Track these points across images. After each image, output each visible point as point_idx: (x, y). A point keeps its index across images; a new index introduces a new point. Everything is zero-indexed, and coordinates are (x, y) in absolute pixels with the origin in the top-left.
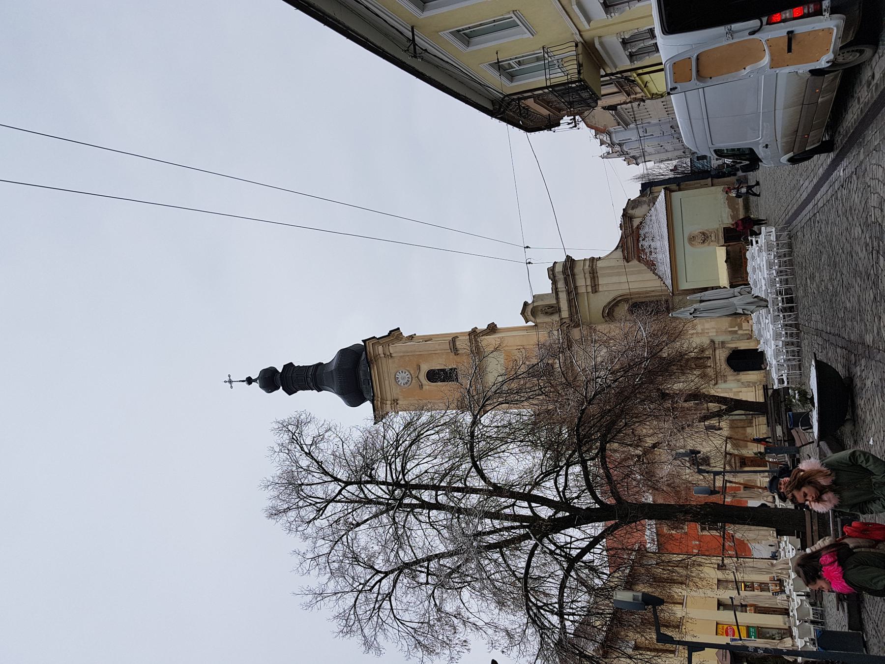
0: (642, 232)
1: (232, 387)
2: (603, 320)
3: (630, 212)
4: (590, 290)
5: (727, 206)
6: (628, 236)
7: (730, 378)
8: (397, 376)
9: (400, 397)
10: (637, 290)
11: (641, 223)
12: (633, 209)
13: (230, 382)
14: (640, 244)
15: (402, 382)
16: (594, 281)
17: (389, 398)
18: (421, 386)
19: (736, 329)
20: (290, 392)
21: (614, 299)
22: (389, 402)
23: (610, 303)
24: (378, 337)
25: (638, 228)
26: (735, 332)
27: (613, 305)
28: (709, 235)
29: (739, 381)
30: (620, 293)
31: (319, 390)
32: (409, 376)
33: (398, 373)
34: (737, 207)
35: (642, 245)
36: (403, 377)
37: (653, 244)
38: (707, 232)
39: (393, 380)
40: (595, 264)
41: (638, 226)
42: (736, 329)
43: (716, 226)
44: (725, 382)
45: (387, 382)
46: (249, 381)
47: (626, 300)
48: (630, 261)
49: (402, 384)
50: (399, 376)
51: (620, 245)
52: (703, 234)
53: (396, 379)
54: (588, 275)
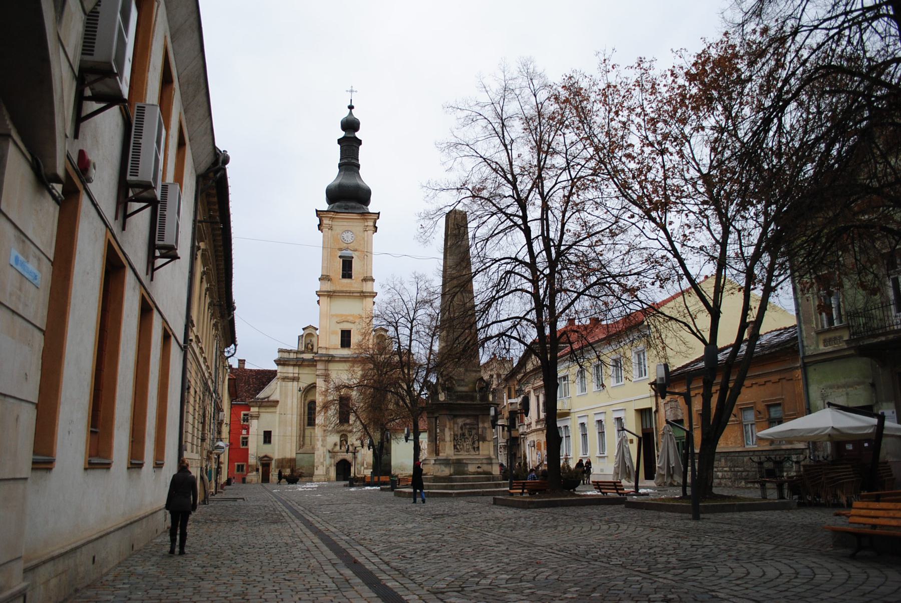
1: (347, 91)
7: (333, 461)
9: (333, 232)
13: (352, 91)
15: (345, 235)
17: (334, 223)
18: (341, 249)
19: (365, 466)
20: (340, 141)
22: (330, 222)
24: (377, 221)
26: (363, 465)
29: (331, 465)
31: (340, 166)
36: (348, 237)
42: (365, 466)
44: (331, 457)
45: (345, 224)
46: (351, 107)
50: (349, 234)
53: (348, 231)
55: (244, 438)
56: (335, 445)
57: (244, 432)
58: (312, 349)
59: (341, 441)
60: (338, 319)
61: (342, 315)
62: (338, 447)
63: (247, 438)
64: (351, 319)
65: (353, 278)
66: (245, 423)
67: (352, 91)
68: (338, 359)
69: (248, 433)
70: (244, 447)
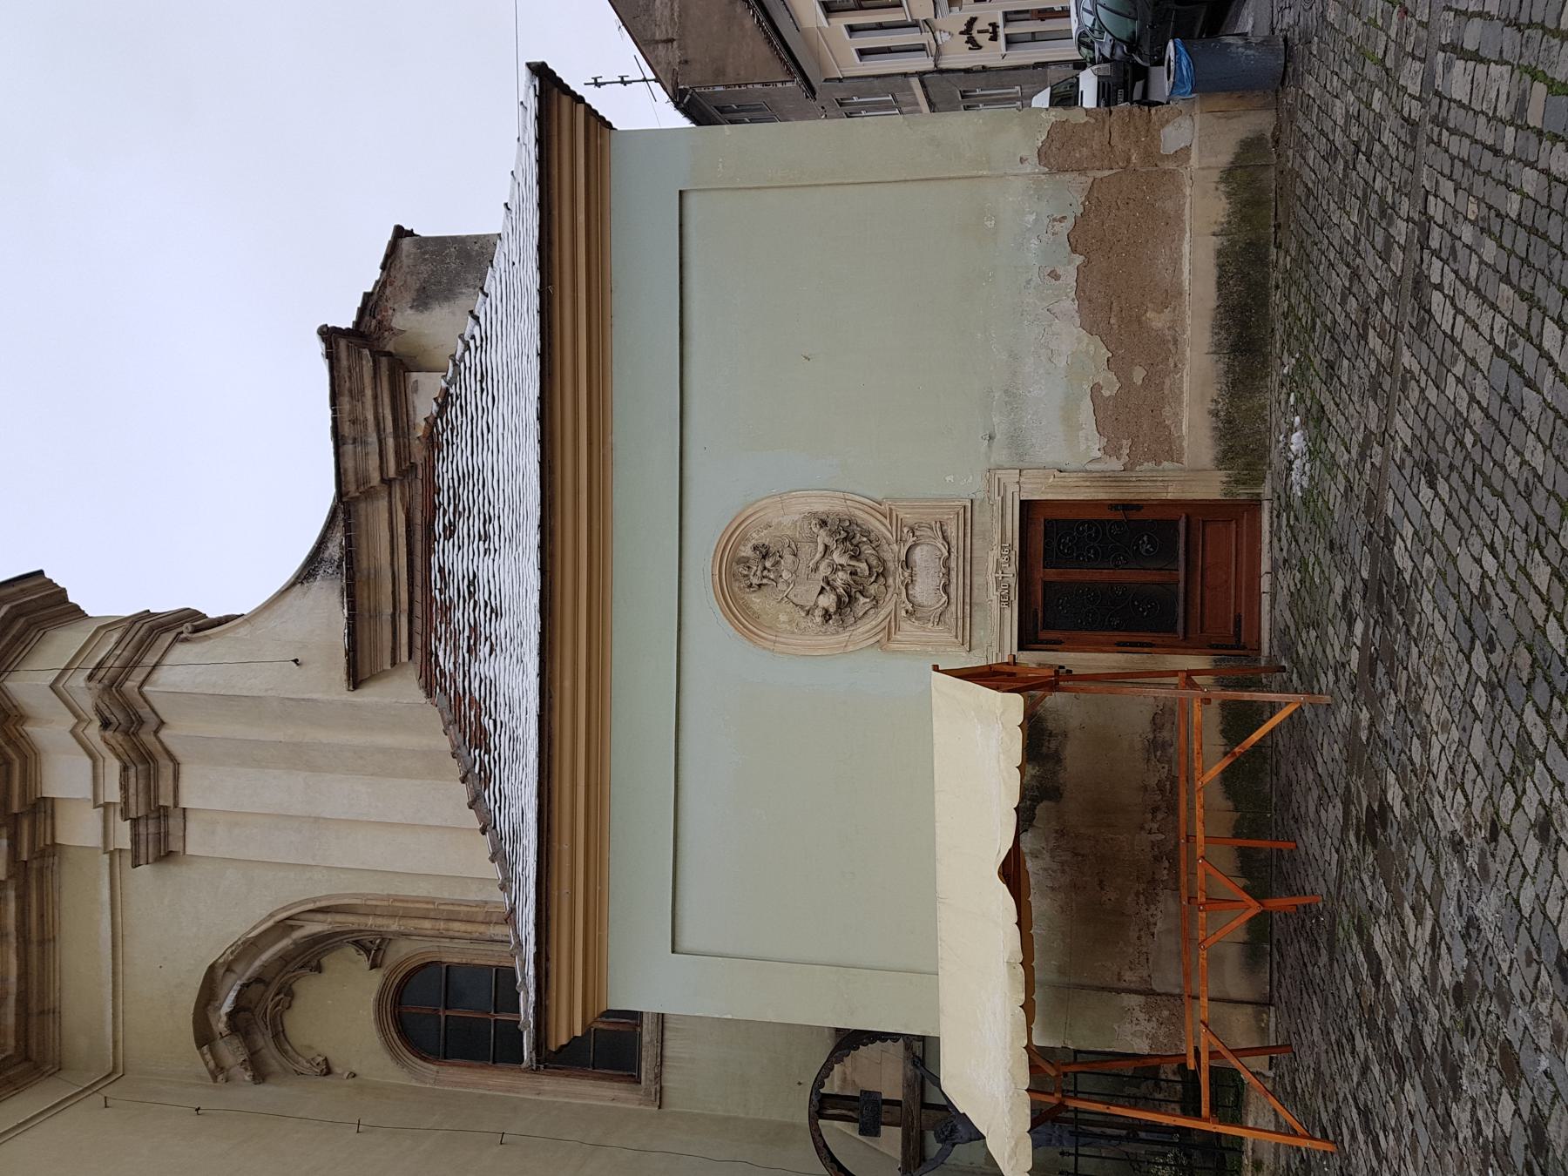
0: (446, 473)
2: (193, 1060)
3: (405, 320)
4: (122, 835)
5: (1069, 305)
6: (369, 494)
10: (423, 890)
11: (444, 401)
12: (423, 300)
14: (434, 560)
16: (151, 789)
21: (285, 926)
23: (249, 947)
25: (433, 442)
27: (284, 959)
28: (893, 553)
30: (322, 889)
34: (1157, 320)
35: (441, 570)
37: (485, 568)
38: (876, 525)
40: (150, 659)
41: (431, 423)
43: (965, 483)
47: (373, 948)
48: (376, 676)
51: (334, 550)
52: (848, 534)
54: (93, 732)
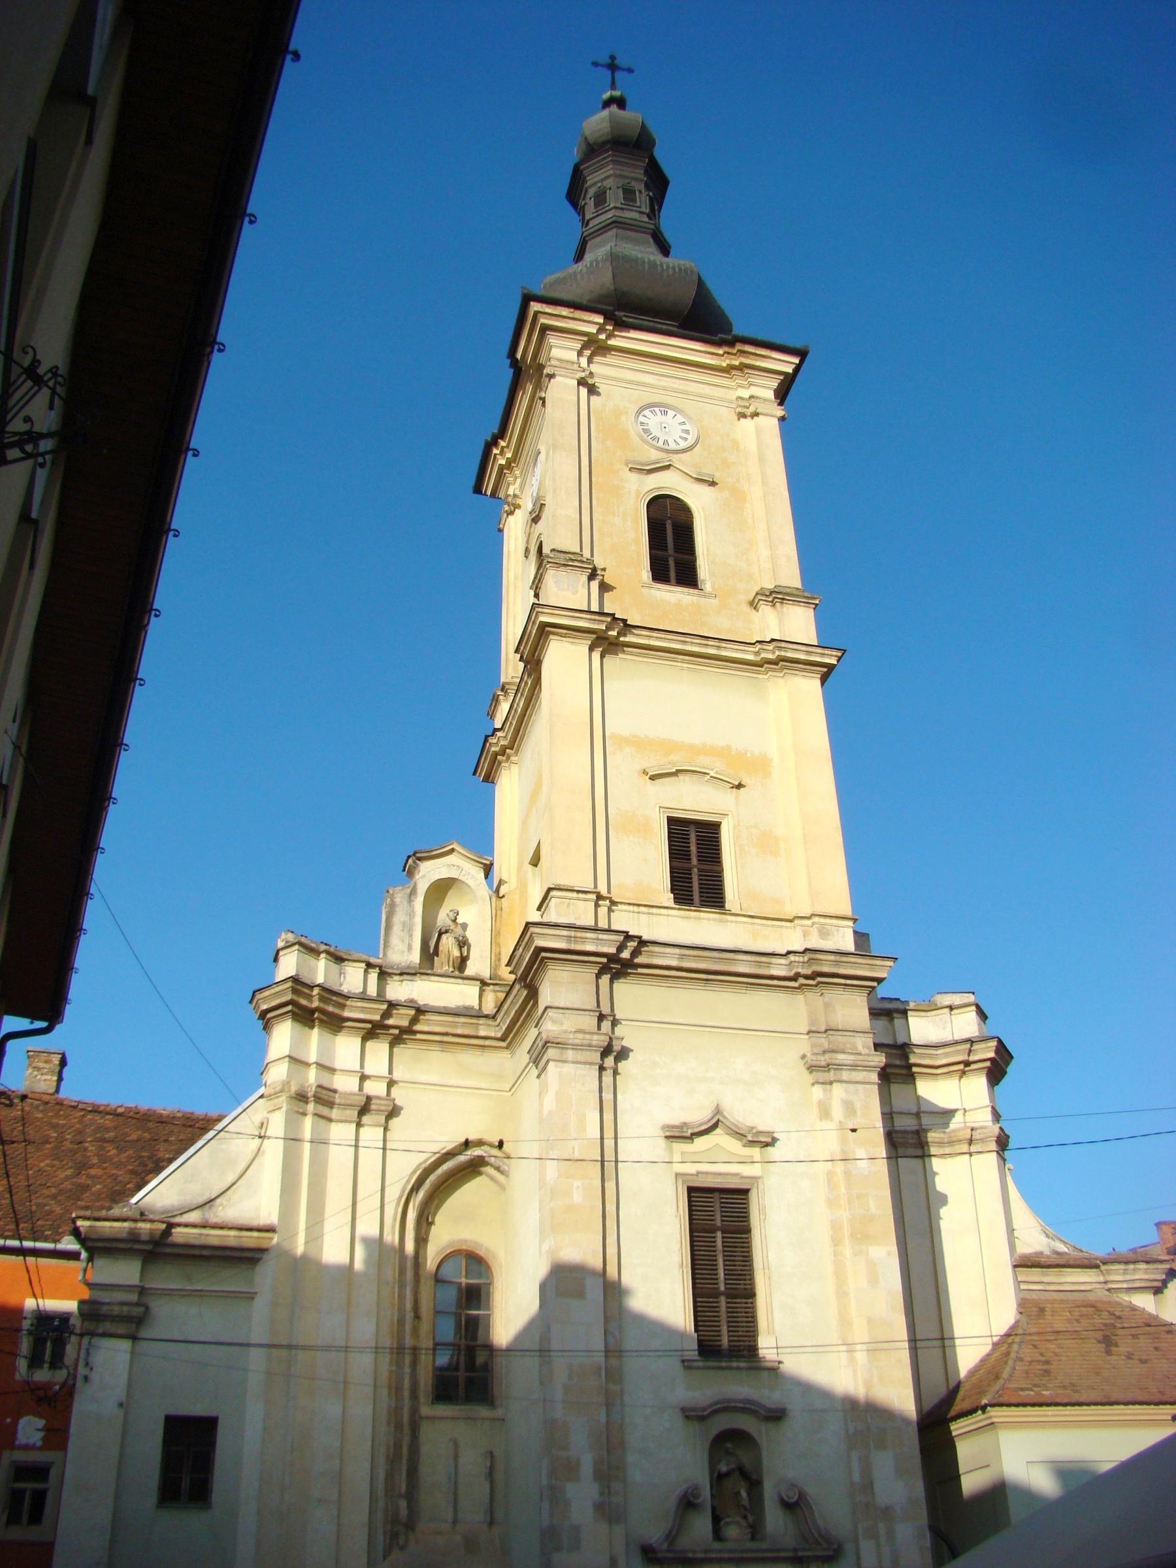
8: (671, 413)
32: (673, 446)
33: (680, 418)
39: (657, 399)
49: (641, 419)
50: (672, 421)
53: (664, 408)
55: (25, 1472)
56: (688, 1503)
57: (30, 1429)
58: (463, 961)
59: (718, 1479)
60: (656, 764)
61: (669, 747)
62: (701, 1526)
63: (40, 1472)
64: (715, 766)
65: (708, 587)
66: (42, 1375)
67: (613, 67)
68: (670, 958)
69: (57, 1436)
70: (17, 1533)
